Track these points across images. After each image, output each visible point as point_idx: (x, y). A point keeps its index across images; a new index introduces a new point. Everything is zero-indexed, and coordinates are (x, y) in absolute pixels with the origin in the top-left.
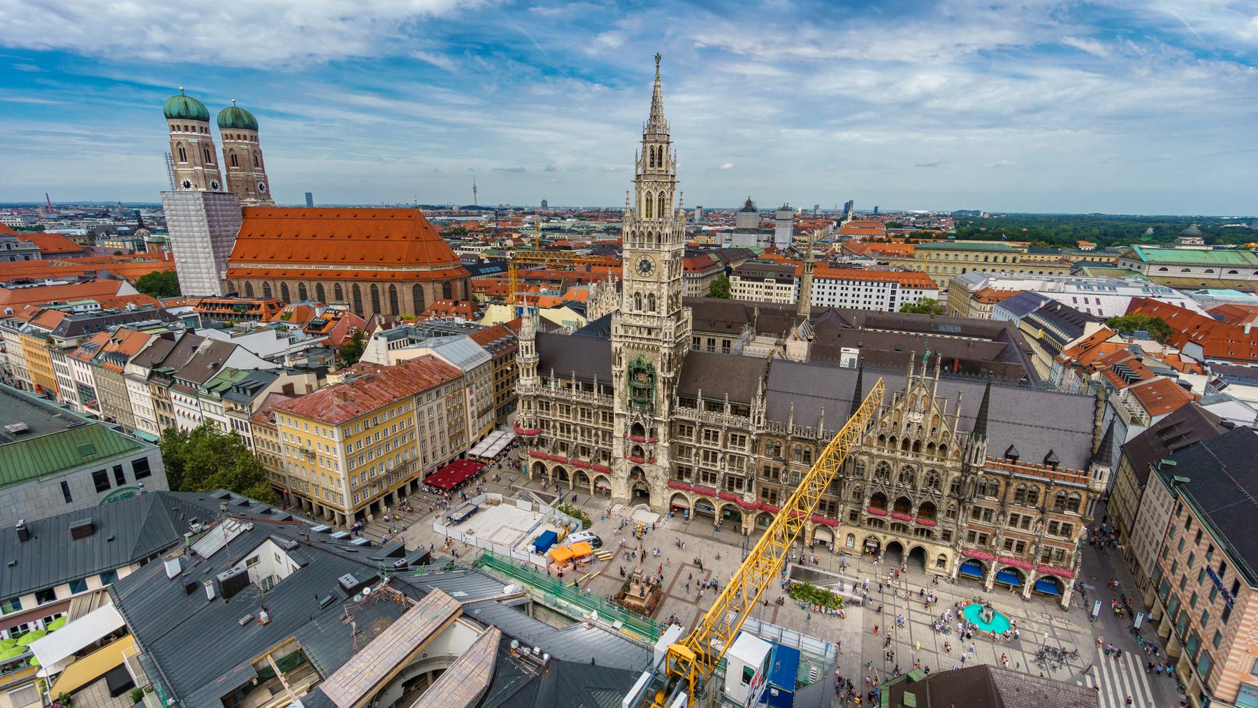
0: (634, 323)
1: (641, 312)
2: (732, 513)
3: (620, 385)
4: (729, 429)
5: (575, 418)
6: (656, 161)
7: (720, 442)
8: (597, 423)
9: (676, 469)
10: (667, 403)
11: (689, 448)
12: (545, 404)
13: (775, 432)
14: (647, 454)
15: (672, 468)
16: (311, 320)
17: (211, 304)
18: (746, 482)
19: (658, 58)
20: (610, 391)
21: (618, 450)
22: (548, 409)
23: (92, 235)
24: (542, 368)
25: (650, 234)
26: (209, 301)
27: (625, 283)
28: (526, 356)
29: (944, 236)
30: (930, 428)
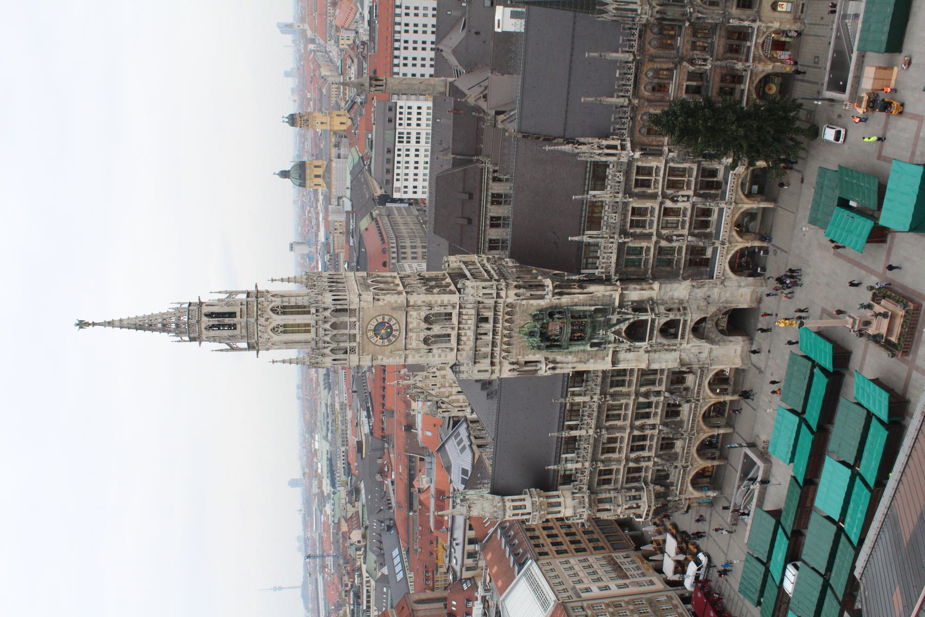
0: (471, 344)
1: (454, 334)
2: (753, 182)
4: (628, 192)
5: (622, 428)
6: (227, 321)
7: (648, 204)
8: (628, 395)
10: (592, 288)
11: (660, 251)
12: (604, 477)
13: (628, 123)
14: (672, 316)
15: (692, 277)
18: (706, 164)
19: (82, 324)
20: (579, 377)
21: (667, 361)
22: (610, 472)
24: (545, 482)
25: (334, 326)
27: (410, 361)
28: (529, 509)
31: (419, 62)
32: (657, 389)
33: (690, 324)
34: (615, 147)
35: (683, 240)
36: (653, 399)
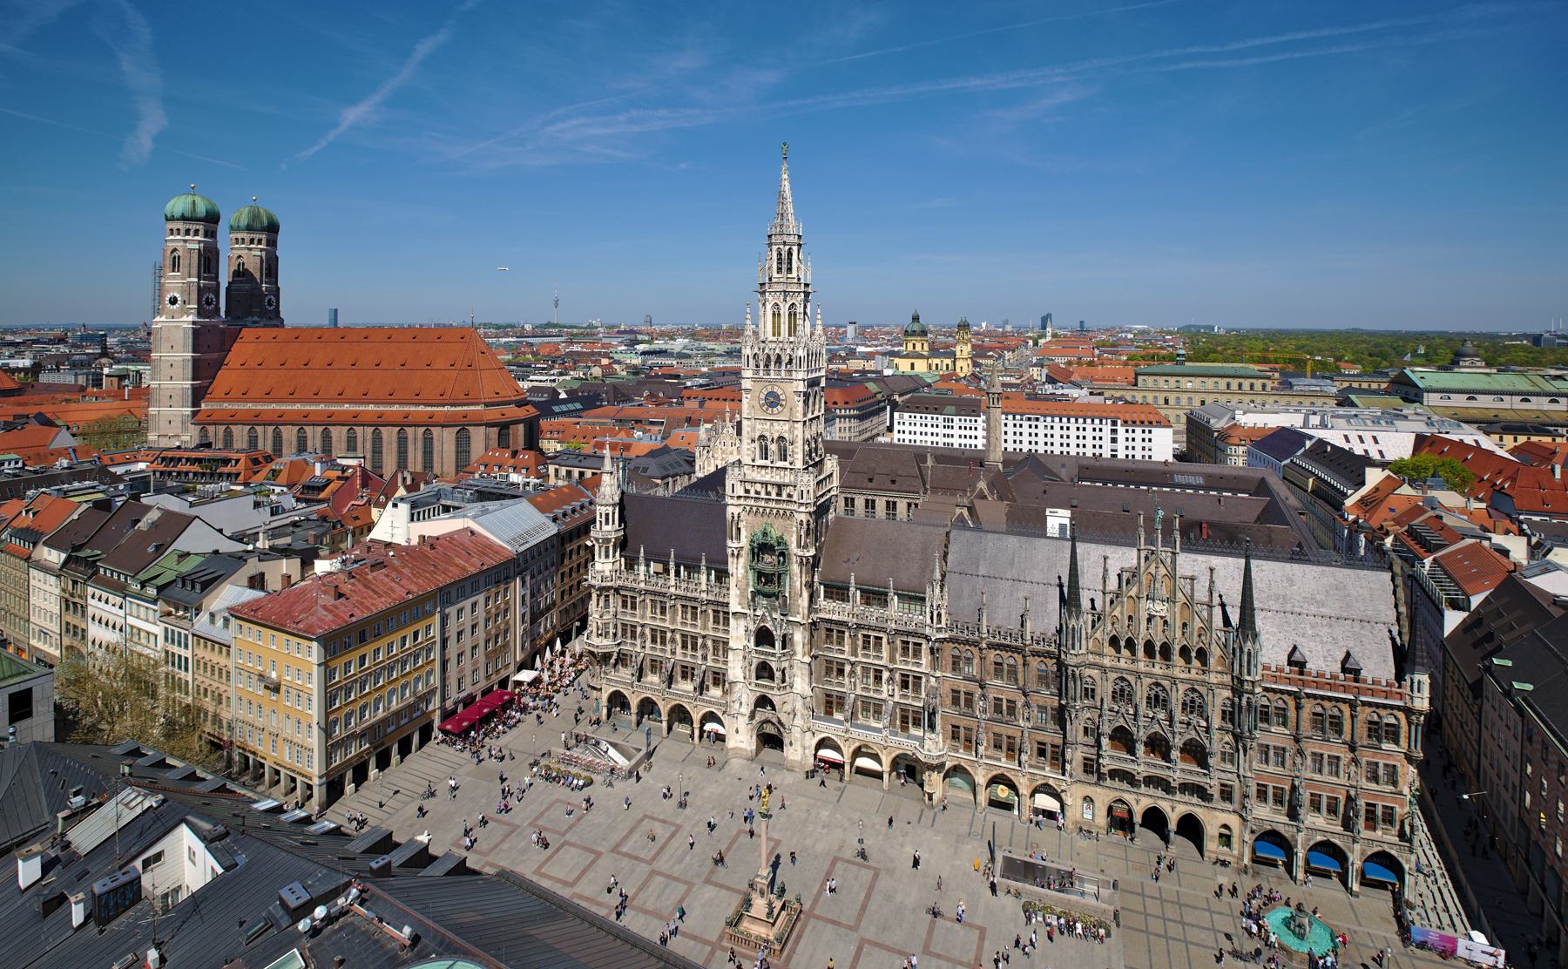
0: (758, 478)
1: (767, 462)
3: (739, 569)
4: (897, 632)
5: (673, 621)
7: (885, 653)
8: (705, 627)
9: (823, 699)
10: (806, 595)
14: (778, 675)
16: (305, 480)
17: (172, 459)
21: (736, 669)
22: (634, 607)
23: (36, 369)
26: (170, 454)
27: (745, 423)
29: (1172, 358)
30: (1179, 624)
31: (1018, 438)
32: (710, 657)
33: (770, 694)
34: (939, 622)
35: (851, 687)
36: (699, 653)
